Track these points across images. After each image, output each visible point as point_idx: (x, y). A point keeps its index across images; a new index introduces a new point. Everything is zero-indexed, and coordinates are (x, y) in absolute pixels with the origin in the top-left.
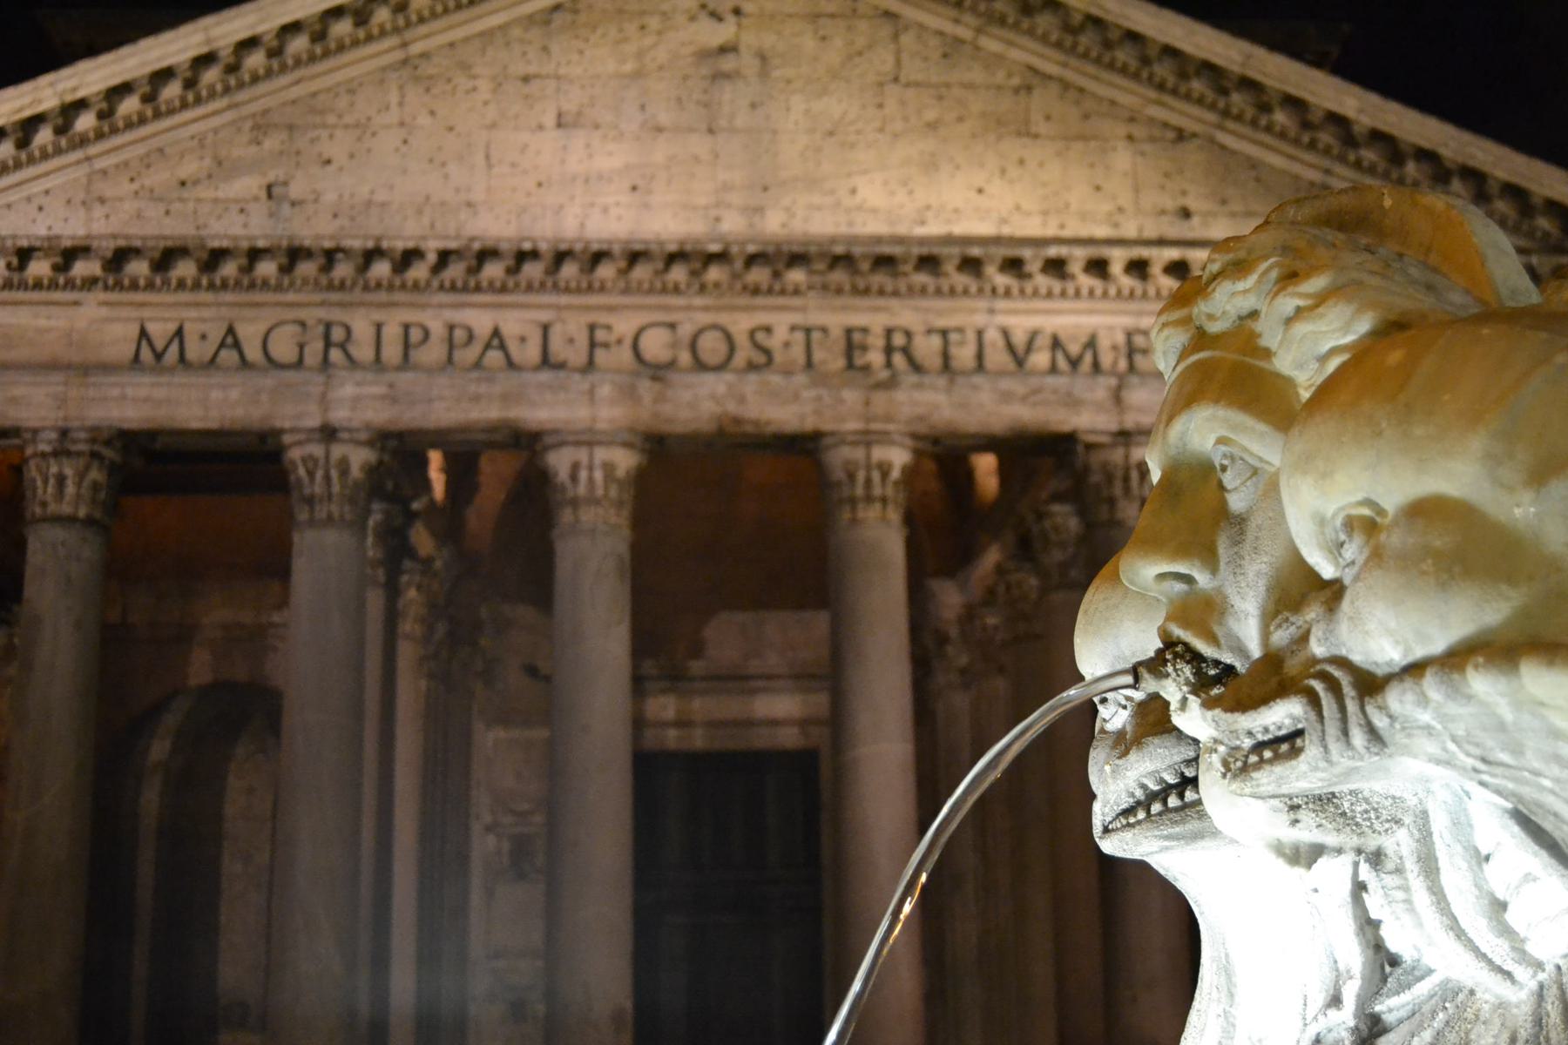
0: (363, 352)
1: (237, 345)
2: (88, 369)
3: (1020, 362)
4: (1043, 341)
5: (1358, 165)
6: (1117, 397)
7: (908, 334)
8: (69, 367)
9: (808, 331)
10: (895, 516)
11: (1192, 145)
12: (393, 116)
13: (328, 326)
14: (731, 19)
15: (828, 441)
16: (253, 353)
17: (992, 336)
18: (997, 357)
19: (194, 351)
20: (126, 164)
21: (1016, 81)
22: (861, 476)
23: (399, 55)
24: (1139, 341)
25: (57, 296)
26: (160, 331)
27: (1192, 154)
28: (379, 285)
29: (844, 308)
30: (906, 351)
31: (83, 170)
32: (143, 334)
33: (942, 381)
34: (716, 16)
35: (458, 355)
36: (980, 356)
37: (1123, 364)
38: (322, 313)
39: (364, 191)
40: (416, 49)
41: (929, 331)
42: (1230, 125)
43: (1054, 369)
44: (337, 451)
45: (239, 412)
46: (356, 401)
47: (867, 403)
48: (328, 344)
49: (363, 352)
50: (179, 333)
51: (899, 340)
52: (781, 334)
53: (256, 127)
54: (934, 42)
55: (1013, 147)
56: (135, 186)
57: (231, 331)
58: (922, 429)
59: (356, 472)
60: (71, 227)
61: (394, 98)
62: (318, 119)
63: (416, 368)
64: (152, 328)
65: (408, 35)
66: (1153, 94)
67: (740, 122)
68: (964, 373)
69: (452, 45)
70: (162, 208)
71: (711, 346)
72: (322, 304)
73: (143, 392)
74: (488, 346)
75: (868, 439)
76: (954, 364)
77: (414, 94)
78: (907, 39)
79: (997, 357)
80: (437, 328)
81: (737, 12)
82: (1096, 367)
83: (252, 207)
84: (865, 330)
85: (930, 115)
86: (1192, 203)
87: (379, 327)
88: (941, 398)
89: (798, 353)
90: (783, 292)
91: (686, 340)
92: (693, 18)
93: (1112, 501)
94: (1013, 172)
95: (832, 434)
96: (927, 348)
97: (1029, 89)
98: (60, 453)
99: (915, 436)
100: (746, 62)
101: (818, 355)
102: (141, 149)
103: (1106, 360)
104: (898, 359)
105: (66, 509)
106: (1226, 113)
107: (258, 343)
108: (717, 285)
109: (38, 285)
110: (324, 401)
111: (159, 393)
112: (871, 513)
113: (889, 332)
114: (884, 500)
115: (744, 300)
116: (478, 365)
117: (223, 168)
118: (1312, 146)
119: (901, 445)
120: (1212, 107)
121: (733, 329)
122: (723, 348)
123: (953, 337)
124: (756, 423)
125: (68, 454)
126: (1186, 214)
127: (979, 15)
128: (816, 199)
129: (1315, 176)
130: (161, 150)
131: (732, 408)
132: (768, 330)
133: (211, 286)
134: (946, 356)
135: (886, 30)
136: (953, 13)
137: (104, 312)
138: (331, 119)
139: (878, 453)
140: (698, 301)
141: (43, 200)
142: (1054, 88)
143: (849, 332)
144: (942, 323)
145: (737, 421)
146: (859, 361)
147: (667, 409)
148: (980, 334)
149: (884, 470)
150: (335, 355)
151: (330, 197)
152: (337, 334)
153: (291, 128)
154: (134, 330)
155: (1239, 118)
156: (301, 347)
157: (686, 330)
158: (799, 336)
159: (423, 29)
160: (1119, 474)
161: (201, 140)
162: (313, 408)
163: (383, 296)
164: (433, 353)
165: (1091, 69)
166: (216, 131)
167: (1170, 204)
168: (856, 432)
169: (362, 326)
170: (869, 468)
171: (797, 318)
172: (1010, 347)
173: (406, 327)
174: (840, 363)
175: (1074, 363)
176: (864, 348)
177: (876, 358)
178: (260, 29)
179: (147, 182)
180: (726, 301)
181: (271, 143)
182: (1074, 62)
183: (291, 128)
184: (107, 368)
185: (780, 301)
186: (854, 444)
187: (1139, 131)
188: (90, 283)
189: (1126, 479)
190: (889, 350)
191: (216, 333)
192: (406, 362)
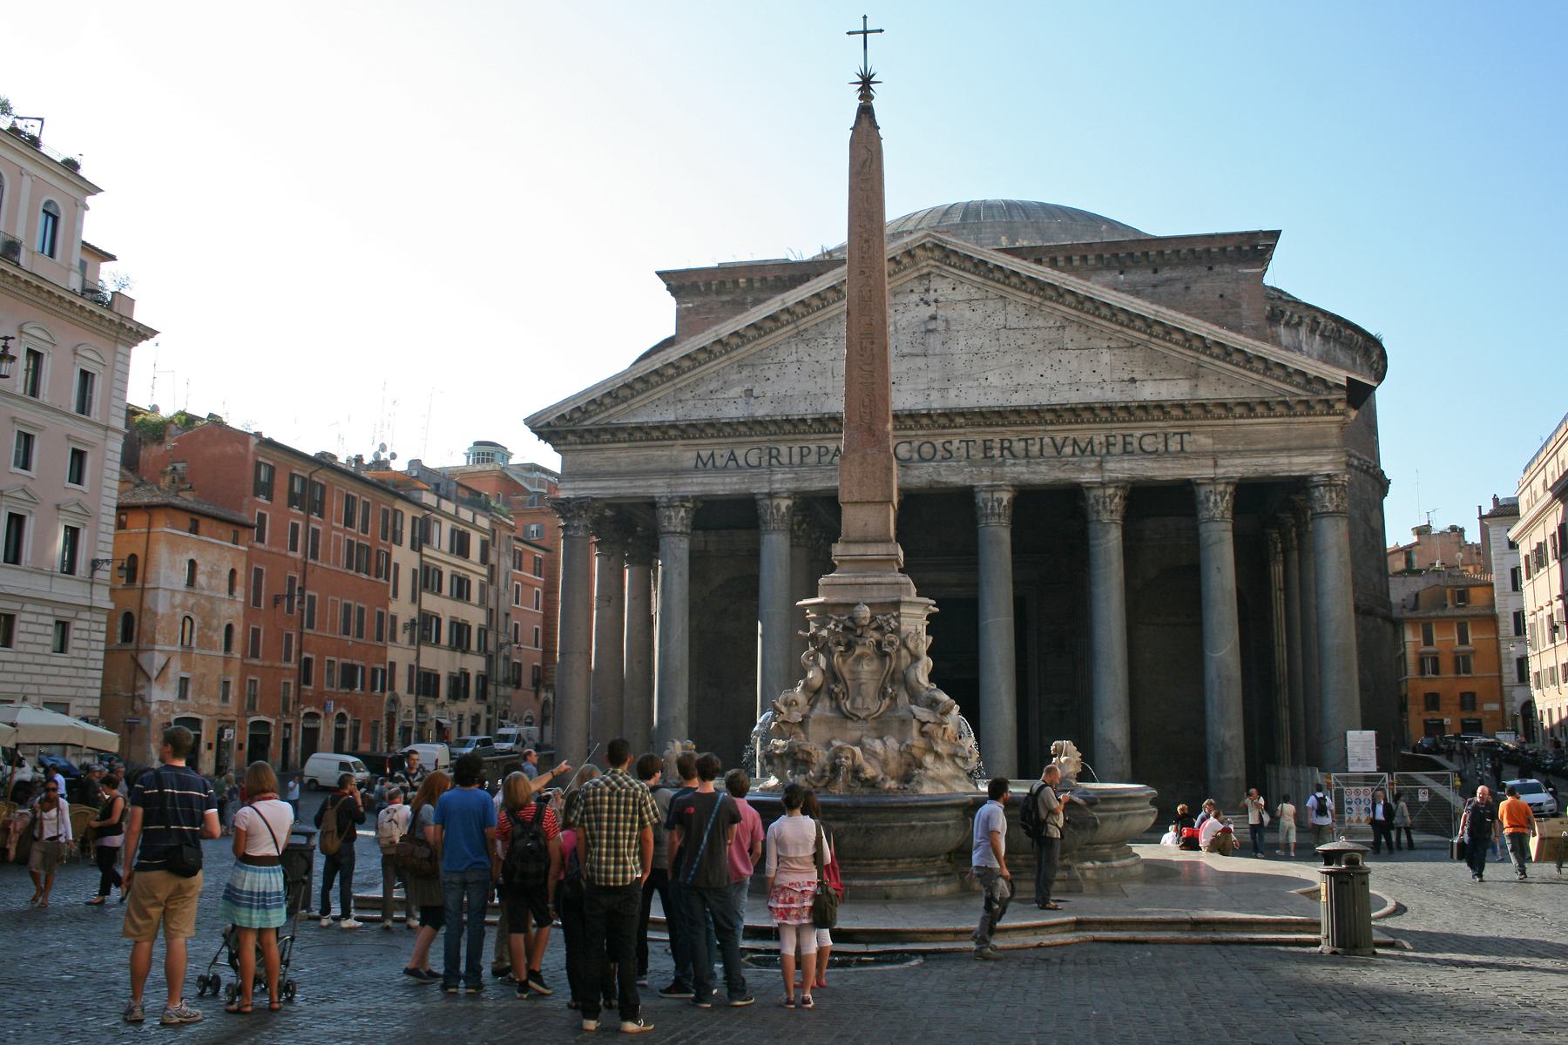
0: (785, 460)
1: (735, 459)
2: (677, 472)
3: (1059, 453)
4: (1070, 442)
5: (1211, 355)
6: (1100, 465)
7: (1011, 442)
8: (672, 471)
9: (967, 442)
10: (1005, 521)
11: (1137, 349)
12: (794, 357)
13: (771, 449)
14: (933, 304)
15: (976, 490)
16: (742, 462)
17: (1047, 440)
18: (1049, 451)
19: (719, 462)
20: (689, 385)
21: (1058, 324)
22: (990, 504)
23: (796, 331)
24: (1111, 439)
25: (666, 443)
26: (705, 454)
27: (1138, 354)
28: (790, 432)
29: (982, 432)
30: (1009, 449)
31: (673, 388)
32: (699, 456)
33: (1024, 461)
34: (927, 303)
35: (823, 459)
36: (1041, 450)
37: (1104, 451)
38: (768, 445)
39: (783, 392)
40: (802, 328)
41: (1020, 440)
42: (1154, 340)
43: (1074, 455)
44: (775, 502)
45: (737, 487)
46: (782, 481)
47: (992, 473)
48: (771, 457)
49: (785, 460)
50: (712, 455)
51: (1006, 444)
52: (956, 443)
53: (739, 366)
54: (1022, 309)
55: (1057, 355)
56: (693, 394)
57: (732, 453)
58: (1016, 483)
59: (783, 509)
60: (669, 416)
61: (794, 351)
62: (763, 361)
63: (806, 465)
64: (701, 453)
65: (798, 323)
66: (1118, 328)
67: (937, 352)
68: (1034, 458)
69: (817, 325)
70: (703, 402)
71: (926, 449)
72: (770, 441)
73: (700, 480)
74: (835, 455)
75: (993, 488)
76: (1030, 453)
77: (802, 347)
78: (1010, 308)
79: (1049, 451)
80: (813, 447)
81: (936, 301)
82: (1092, 451)
83: (739, 400)
84: (992, 440)
85: (1020, 342)
86: (1136, 376)
87: (790, 448)
88: (1024, 469)
89: (963, 451)
90: (955, 427)
91: (916, 449)
92: (917, 305)
93: (1098, 512)
94: (1056, 366)
95: (977, 486)
96: (1019, 447)
97: (1064, 327)
98: (669, 506)
99: (1013, 486)
100: (940, 325)
101: (971, 454)
102: (694, 379)
103: (1096, 449)
104: (1006, 452)
105: (672, 529)
106: (1151, 335)
107: (743, 457)
108: (927, 425)
109: (658, 439)
110: (771, 482)
111: (706, 480)
112: (994, 520)
113: (1002, 440)
114: (999, 515)
115: (937, 431)
116: (831, 463)
117: (726, 385)
118: (1190, 348)
119: (1008, 491)
120: (1145, 332)
121: (935, 443)
122: (932, 451)
123: (1030, 442)
124: (946, 483)
125: (674, 507)
126: (1133, 380)
127: (1041, 297)
128: (970, 384)
129: (1195, 361)
130: (702, 378)
131: (936, 478)
132: (950, 442)
133: (724, 436)
134: (1027, 450)
135: (1000, 304)
136: (1029, 296)
137: (682, 448)
138: (769, 361)
139: (996, 495)
140: (920, 432)
141: (657, 403)
142: (1075, 327)
143: (985, 441)
144: (1024, 436)
145: (938, 482)
146: (989, 455)
147: (908, 480)
148: (1041, 439)
149: (1000, 501)
150: (774, 461)
151: (769, 394)
152: (774, 452)
153: (753, 365)
154: (694, 454)
155: (1157, 337)
156: (760, 458)
157: (916, 444)
158: (964, 444)
159: (804, 320)
160: (1101, 500)
161: (718, 373)
162: (766, 485)
163: (791, 437)
164: (812, 459)
165: (1090, 318)
166: (723, 368)
167: (1126, 377)
168: (987, 486)
169: (784, 449)
170: (993, 500)
171: (963, 438)
172: (1055, 445)
173: (801, 448)
174: (982, 455)
175: (1083, 452)
176: (991, 448)
177: (996, 453)
178: (737, 329)
179: (698, 392)
180: (932, 432)
181: (744, 373)
182: (1083, 315)
183: (753, 365)
184: (686, 471)
185: (955, 430)
186: (985, 491)
187: (1113, 345)
188: (676, 439)
189: (1104, 503)
190: (1002, 449)
191: (727, 455)
192: (802, 463)
